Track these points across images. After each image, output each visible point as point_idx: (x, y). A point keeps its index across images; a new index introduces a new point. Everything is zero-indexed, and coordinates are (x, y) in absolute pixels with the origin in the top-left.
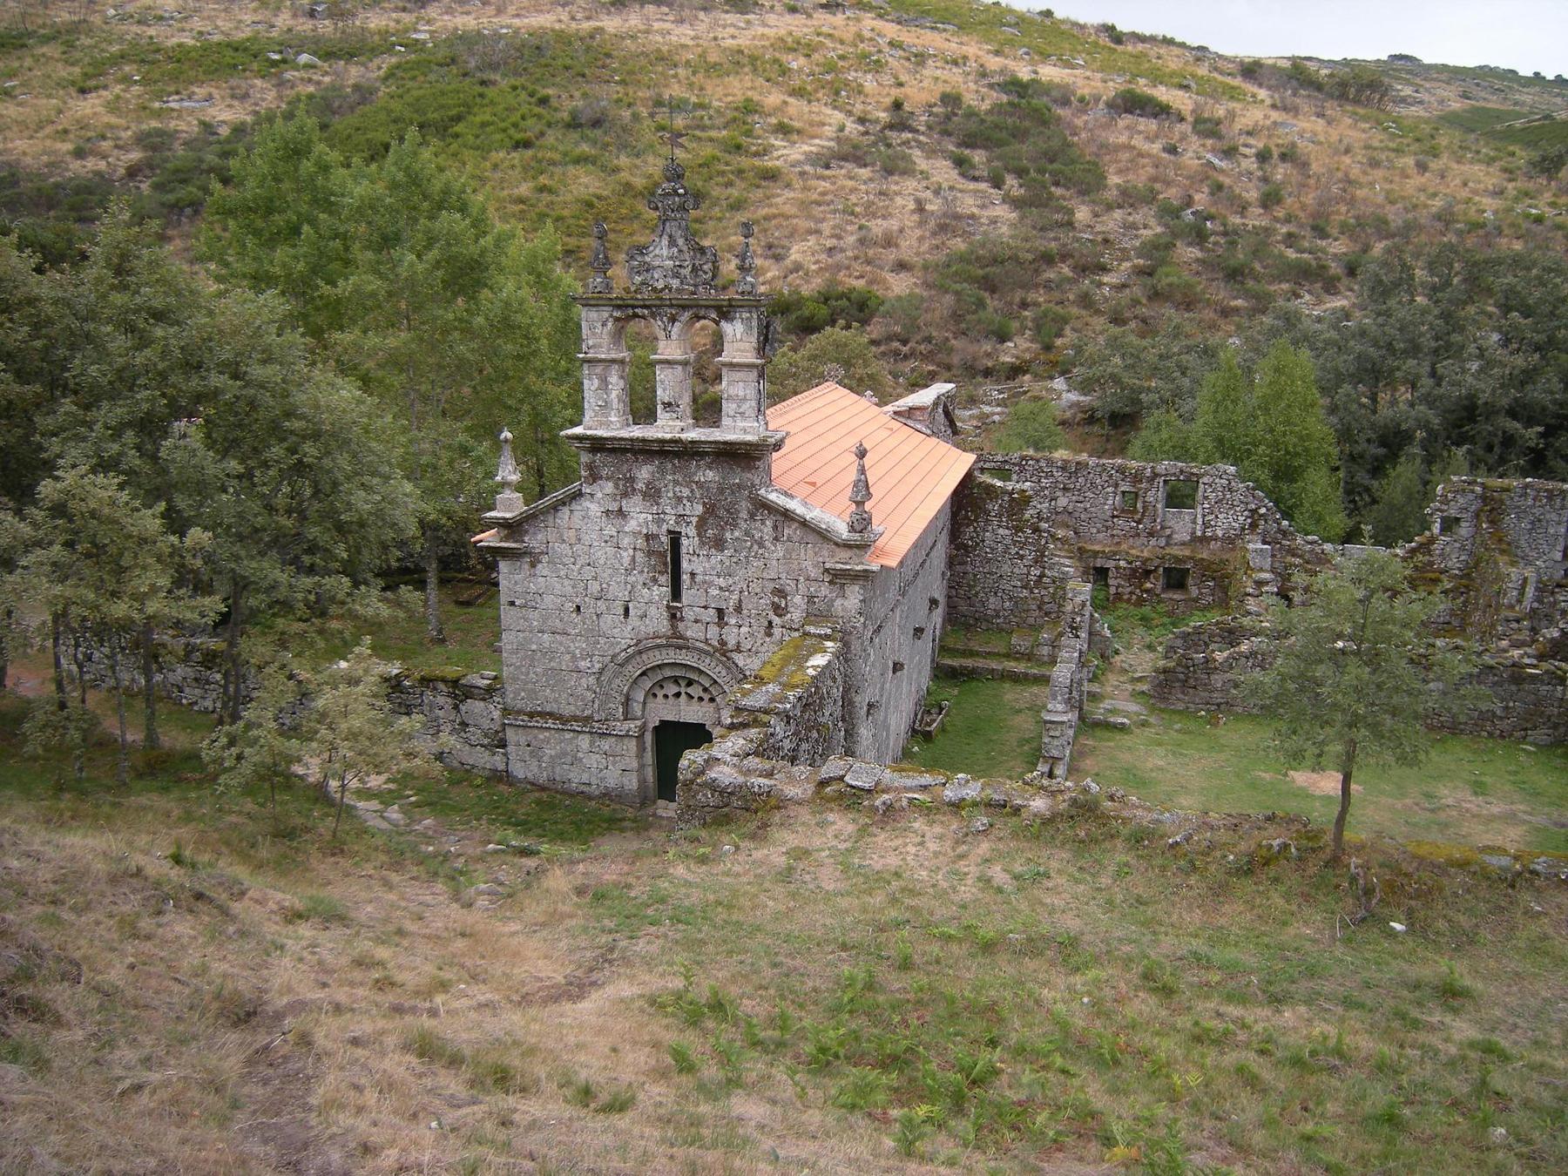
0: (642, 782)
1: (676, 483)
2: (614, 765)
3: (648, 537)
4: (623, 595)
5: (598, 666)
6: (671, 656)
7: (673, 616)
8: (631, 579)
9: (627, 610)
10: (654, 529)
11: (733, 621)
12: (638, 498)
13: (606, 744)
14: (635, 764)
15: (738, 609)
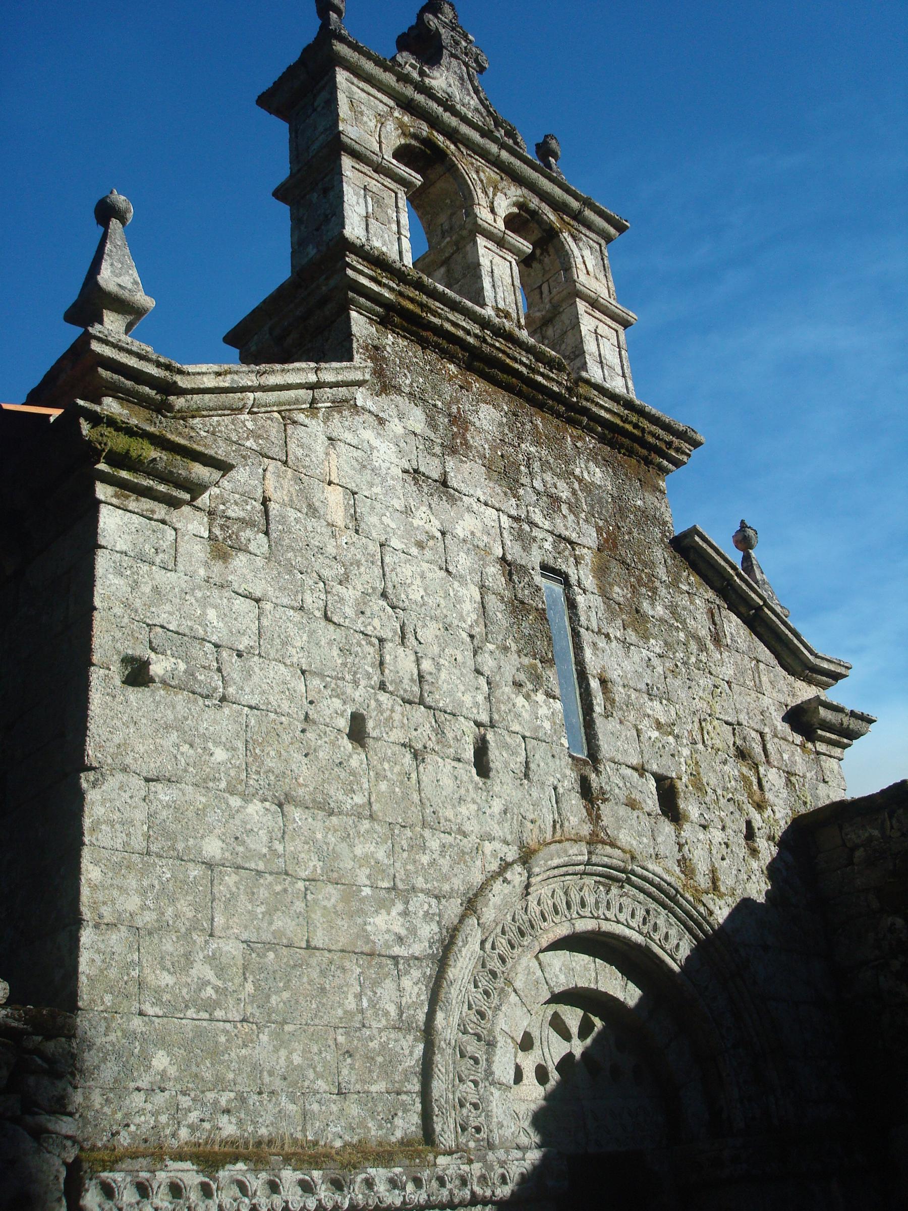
5: (428, 931)
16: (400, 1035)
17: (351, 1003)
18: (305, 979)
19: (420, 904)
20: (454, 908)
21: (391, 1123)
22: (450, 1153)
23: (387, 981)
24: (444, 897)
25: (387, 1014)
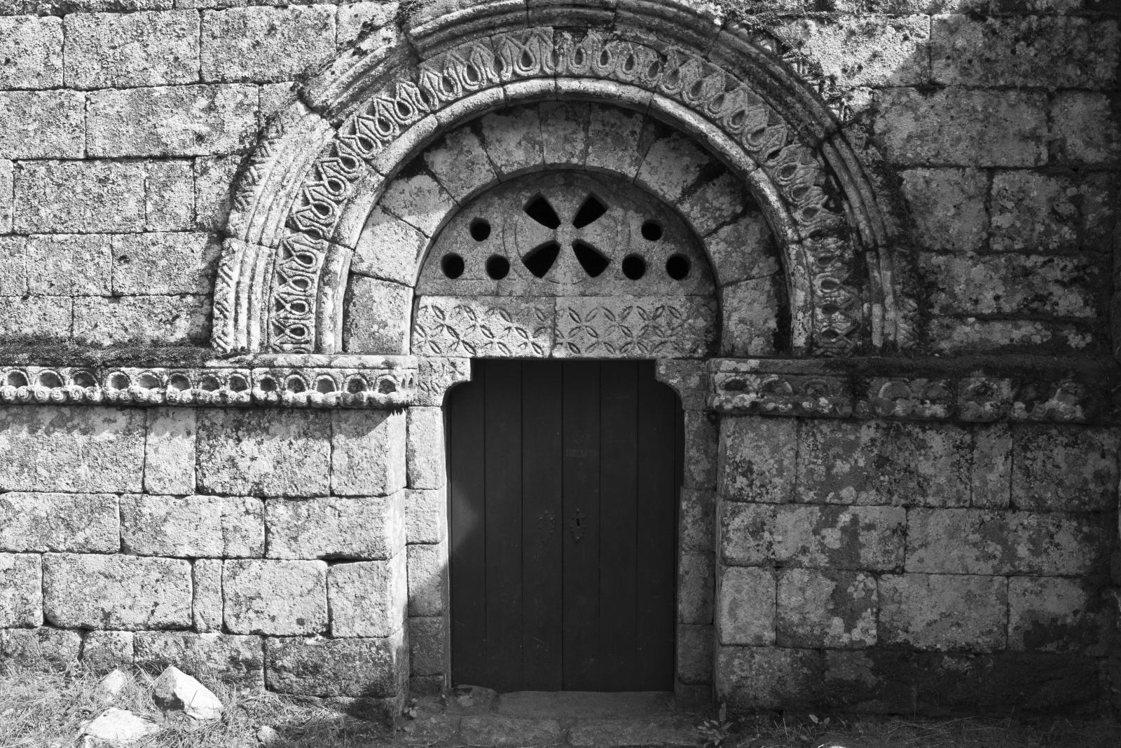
13: (259, 455)
16: (191, 237)
17: (131, 208)
18: (79, 189)
19: (228, 97)
21: (171, 324)
22: (226, 357)
23: (178, 184)
24: (269, 82)
25: (175, 217)
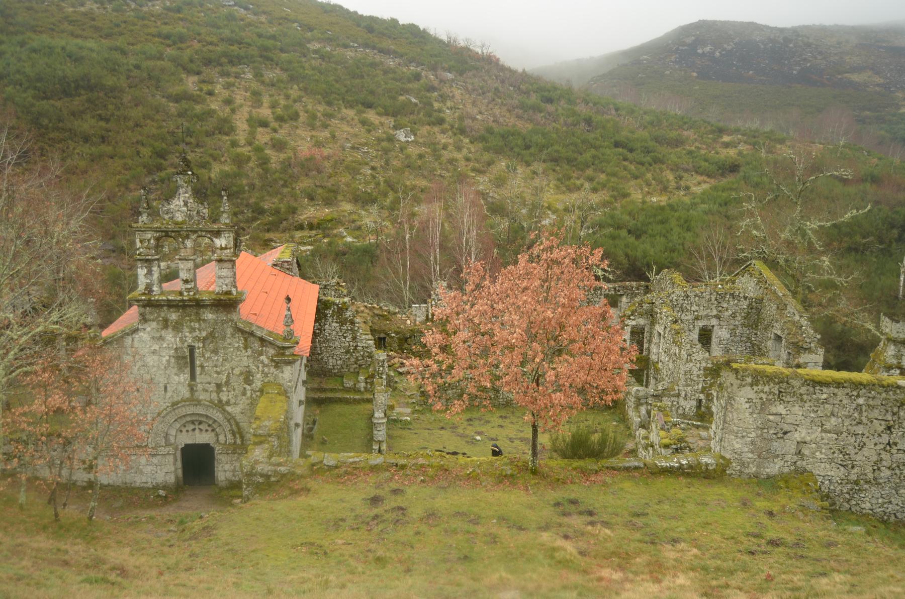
0: (177, 477)
1: (191, 321)
2: (163, 470)
3: (176, 349)
4: (163, 380)
6: (192, 410)
7: (192, 389)
8: (168, 372)
9: (166, 388)
10: (179, 345)
11: (224, 389)
12: (170, 330)
13: (155, 460)
14: (173, 469)
15: (227, 383)
20: (155, 415)
